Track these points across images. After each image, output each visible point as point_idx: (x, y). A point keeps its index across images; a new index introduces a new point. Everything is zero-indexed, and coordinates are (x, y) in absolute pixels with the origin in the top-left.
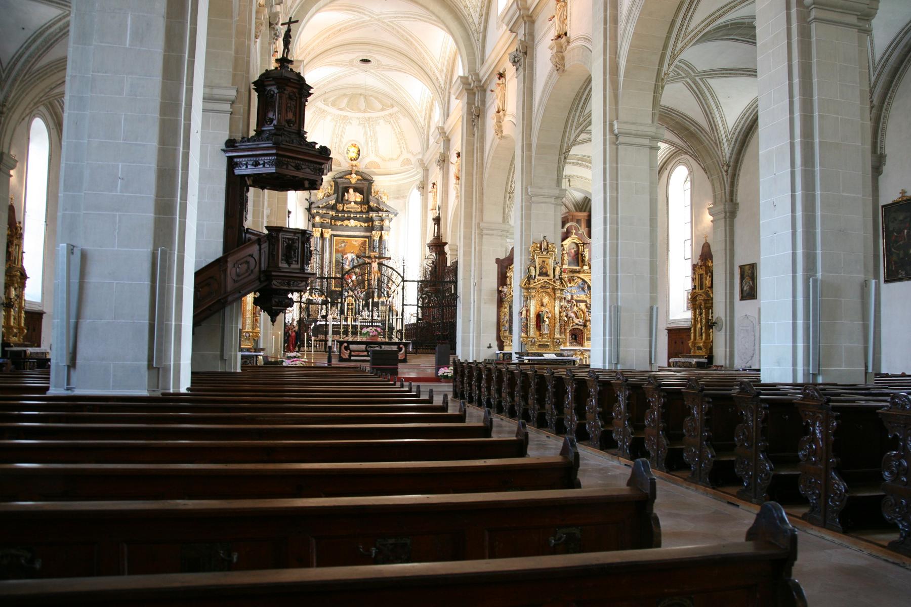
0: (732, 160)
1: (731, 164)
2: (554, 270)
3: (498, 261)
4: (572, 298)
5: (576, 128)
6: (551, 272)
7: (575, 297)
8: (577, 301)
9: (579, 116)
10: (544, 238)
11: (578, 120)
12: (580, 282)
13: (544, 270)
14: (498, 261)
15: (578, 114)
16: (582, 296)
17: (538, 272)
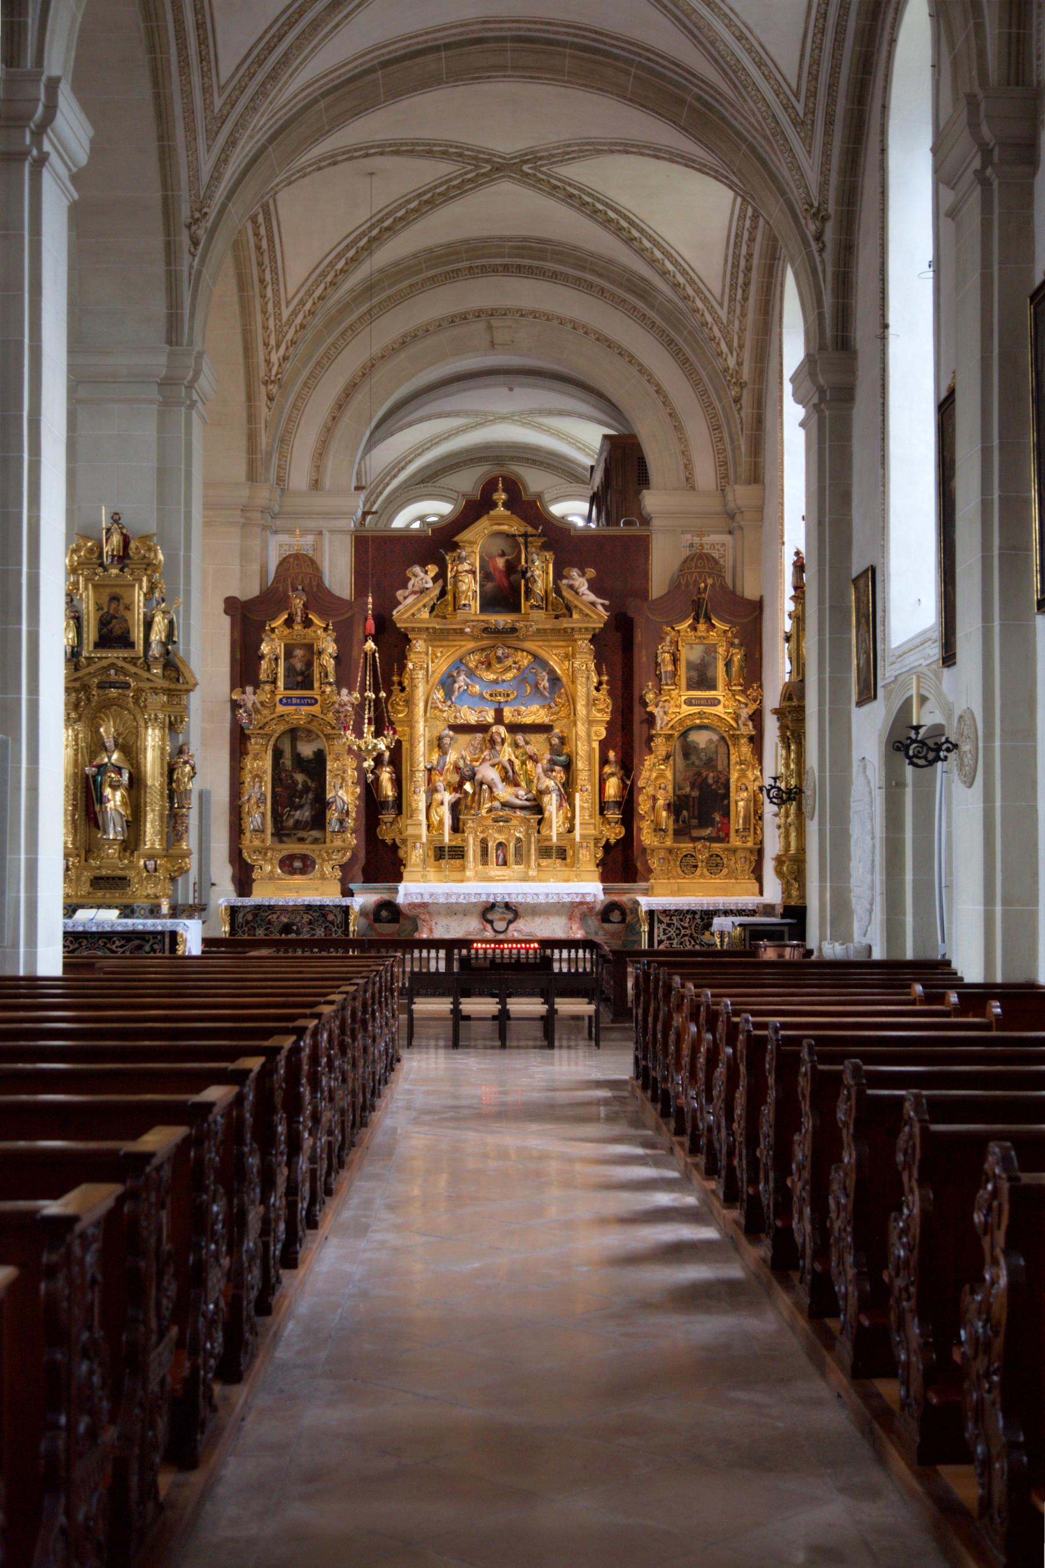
0: (832, 195)
1: (831, 208)
2: (148, 625)
3: (231, 605)
4: (499, 719)
5: (212, 135)
6: (138, 634)
7: (508, 714)
8: (514, 728)
9: (206, 90)
10: (116, 518)
11: (208, 106)
12: (525, 661)
13: (117, 628)
14: (231, 605)
15: (196, 79)
16: (534, 713)
17: (91, 634)
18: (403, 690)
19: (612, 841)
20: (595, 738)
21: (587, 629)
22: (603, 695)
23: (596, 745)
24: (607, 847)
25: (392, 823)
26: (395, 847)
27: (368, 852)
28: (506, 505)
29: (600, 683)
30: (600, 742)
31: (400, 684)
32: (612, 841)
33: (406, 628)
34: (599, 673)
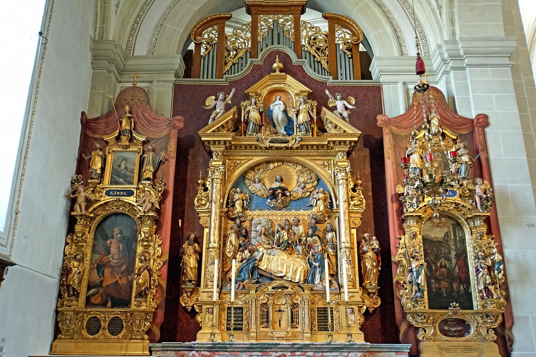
18: (206, 189)
19: (371, 310)
20: (354, 226)
21: (345, 142)
22: (359, 195)
23: (354, 231)
24: (367, 314)
25: (192, 293)
26: (193, 313)
27: (167, 314)
28: (281, 71)
29: (356, 185)
30: (358, 229)
31: (204, 185)
32: (371, 310)
33: (209, 142)
34: (355, 180)
